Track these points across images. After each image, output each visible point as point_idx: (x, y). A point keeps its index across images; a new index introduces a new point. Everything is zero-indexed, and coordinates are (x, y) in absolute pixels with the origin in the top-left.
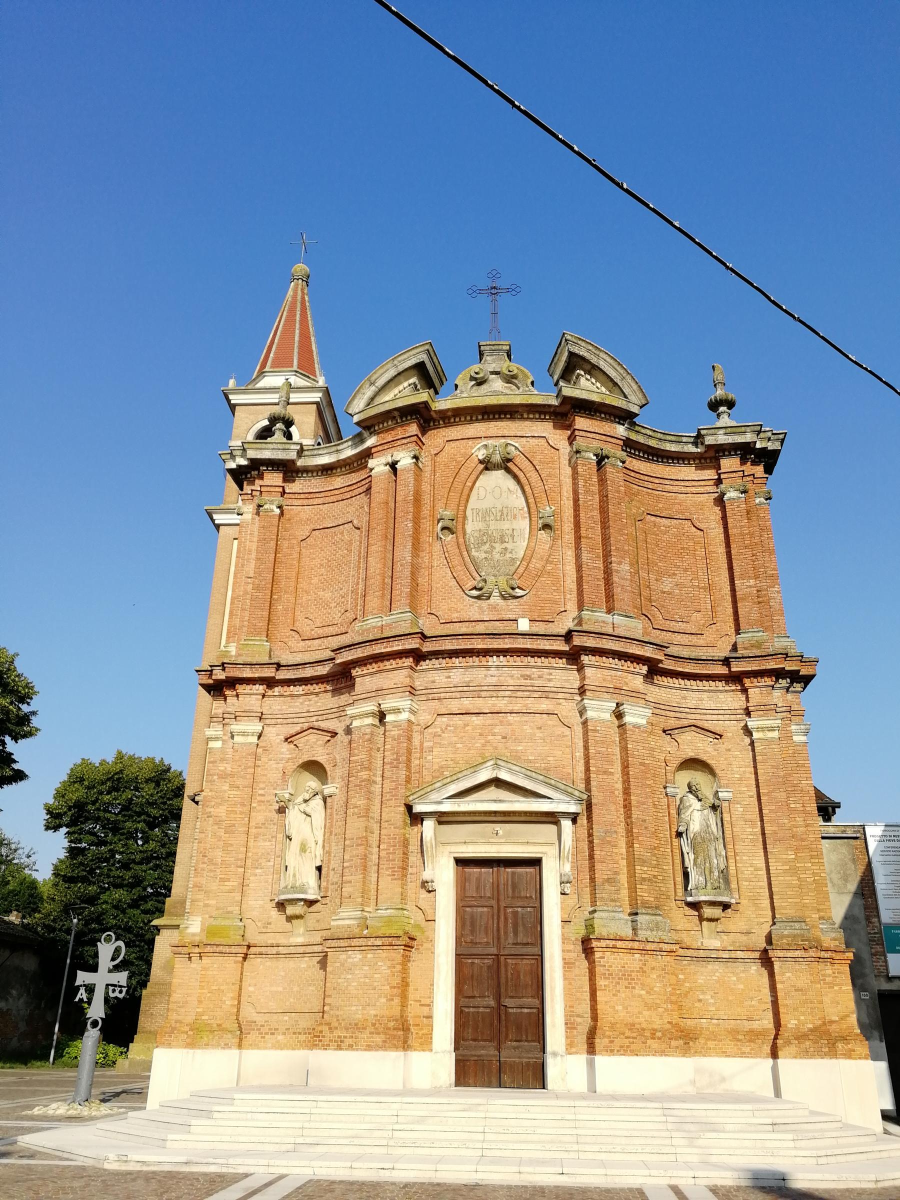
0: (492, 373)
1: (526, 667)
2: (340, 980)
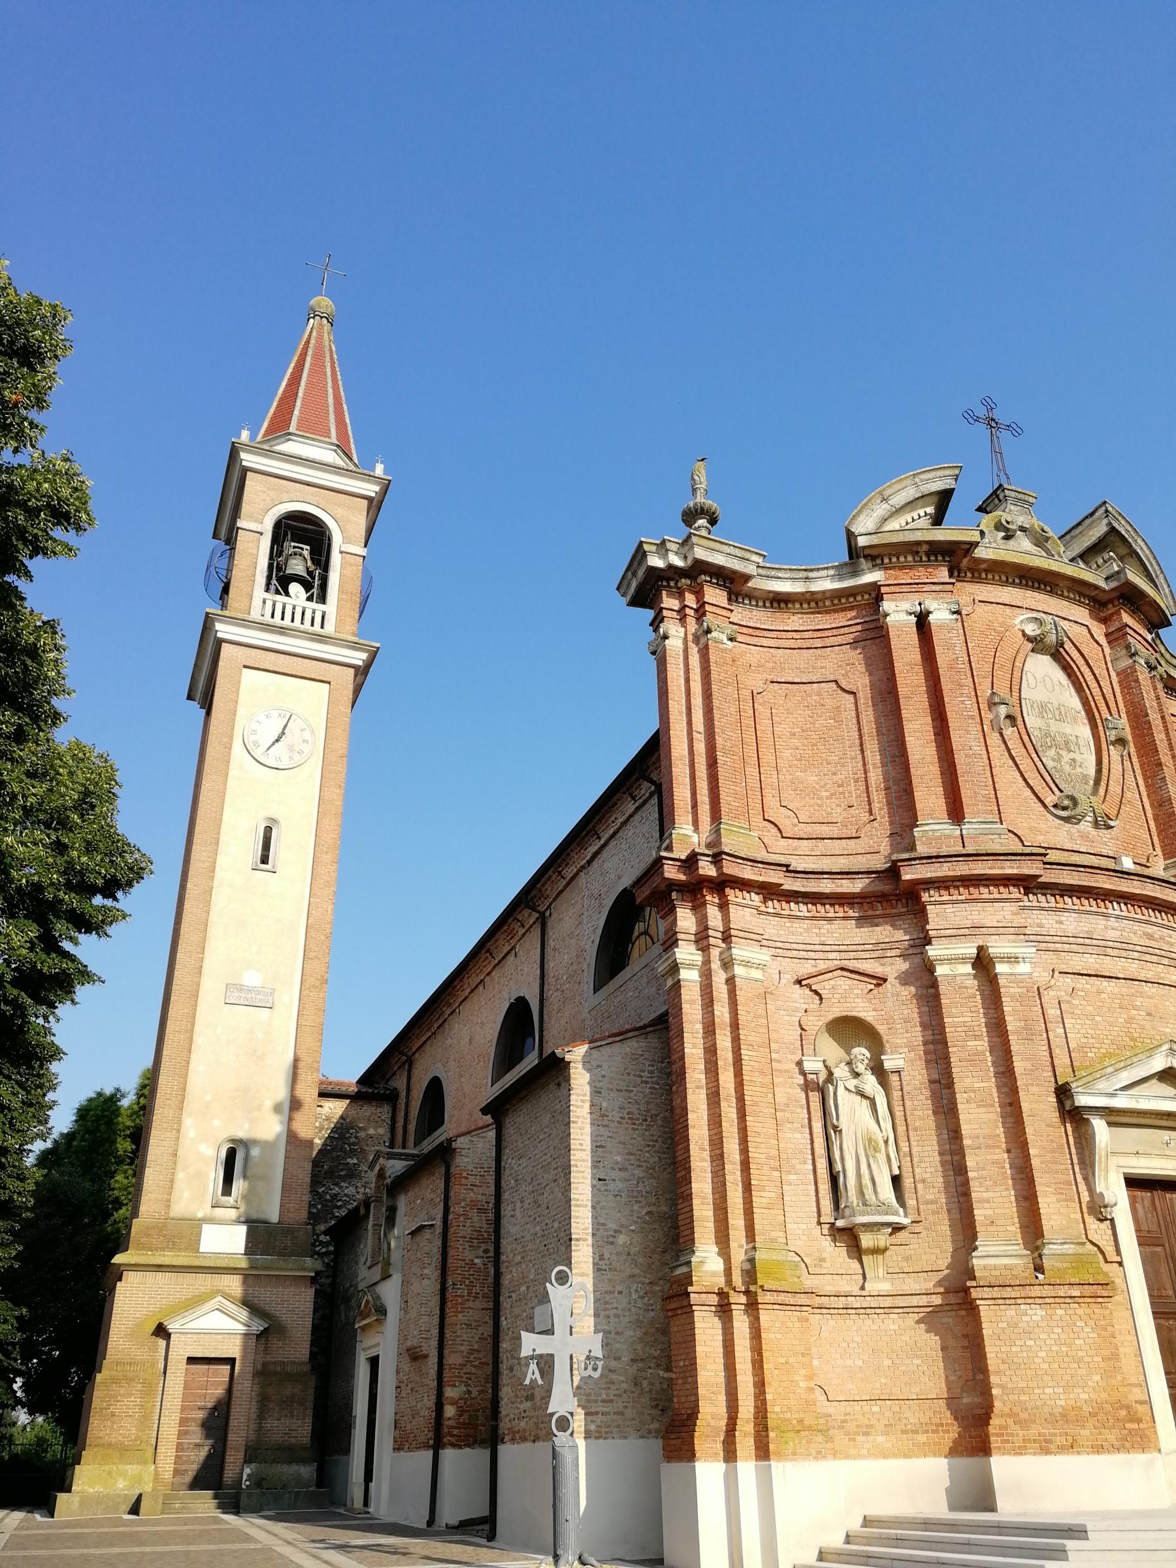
0: (1023, 529)
1: (1147, 922)
2: (1014, 1349)
